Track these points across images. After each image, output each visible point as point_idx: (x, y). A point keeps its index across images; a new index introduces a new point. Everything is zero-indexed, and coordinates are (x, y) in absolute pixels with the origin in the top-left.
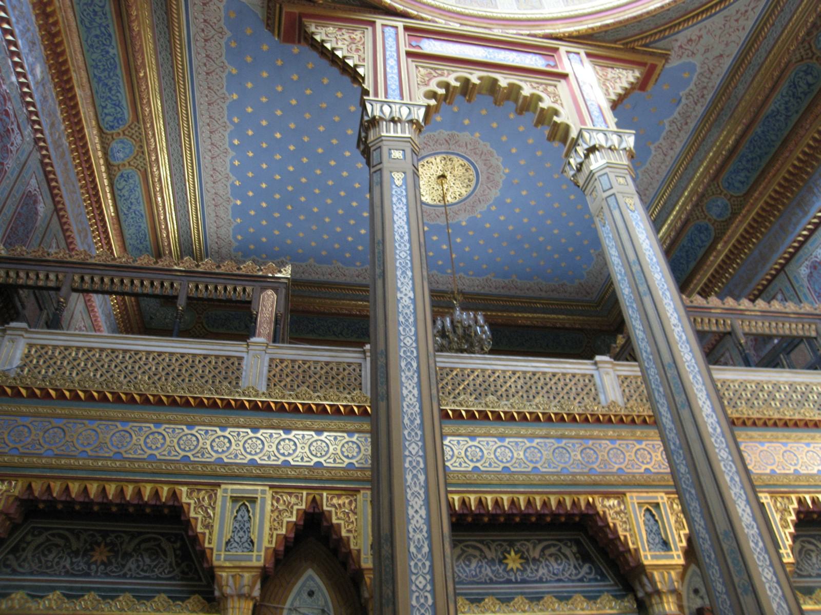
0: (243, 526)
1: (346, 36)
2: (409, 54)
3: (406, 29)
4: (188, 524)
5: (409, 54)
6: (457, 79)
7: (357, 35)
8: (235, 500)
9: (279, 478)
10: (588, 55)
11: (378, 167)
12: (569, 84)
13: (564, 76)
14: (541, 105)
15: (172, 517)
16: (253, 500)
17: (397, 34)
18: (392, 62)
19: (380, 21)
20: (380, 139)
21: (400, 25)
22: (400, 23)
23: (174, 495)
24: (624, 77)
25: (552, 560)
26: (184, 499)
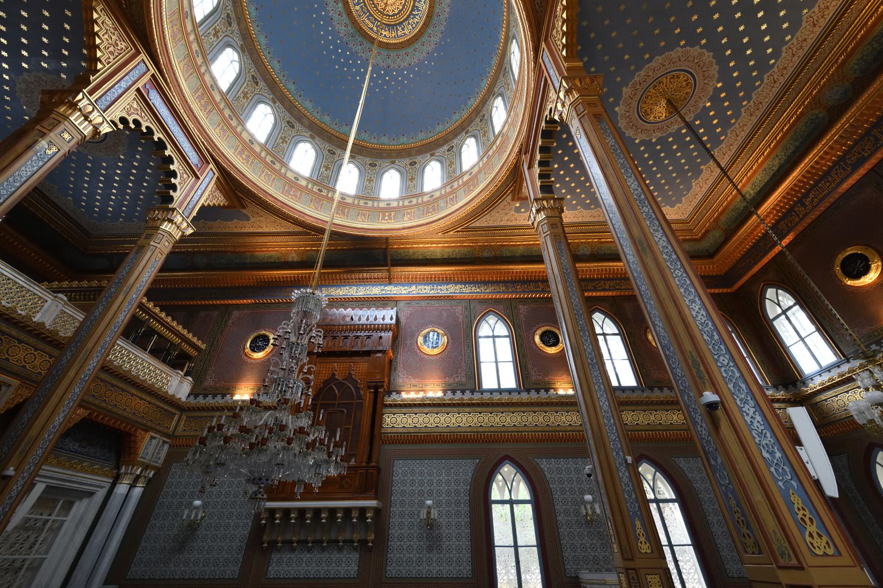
1: (114, 37)
2: (138, 90)
3: (153, 76)
5: (138, 90)
6: (147, 128)
7: (122, 45)
10: (218, 178)
11: (45, 131)
12: (195, 183)
13: (198, 178)
14: (172, 180)
17: (145, 73)
18: (123, 85)
19: (143, 56)
20: (66, 118)
21: (152, 71)
22: (153, 70)
24: (219, 200)
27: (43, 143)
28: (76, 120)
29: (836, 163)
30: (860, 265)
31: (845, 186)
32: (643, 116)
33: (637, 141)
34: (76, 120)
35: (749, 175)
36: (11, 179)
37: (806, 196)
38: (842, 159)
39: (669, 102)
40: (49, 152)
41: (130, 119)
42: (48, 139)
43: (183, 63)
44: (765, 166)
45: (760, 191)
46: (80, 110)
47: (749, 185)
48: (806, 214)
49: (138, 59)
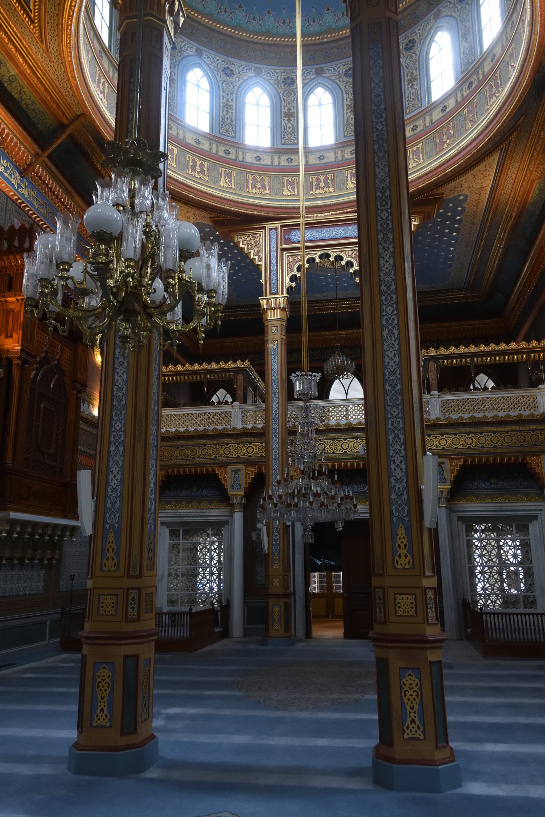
0: (236, 479)
2: (283, 250)
4: (219, 480)
8: (233, 471)
9: (248, 462)
15: (214, 476)
16: (240, 470)
18: (274, 261)
19: (269, 225)
22: (277, 225)
23: (213, 470)
25: (354, 484)
26: (217, 472)
27: (270, 345)
28: (271, 317)
34: (271, 317)
36: (273, 378)
40: (275, 347)
41: (295, 272)
42: (270, 342)
43: (285, 189)
46: (267, 309)
49: (267, 230)
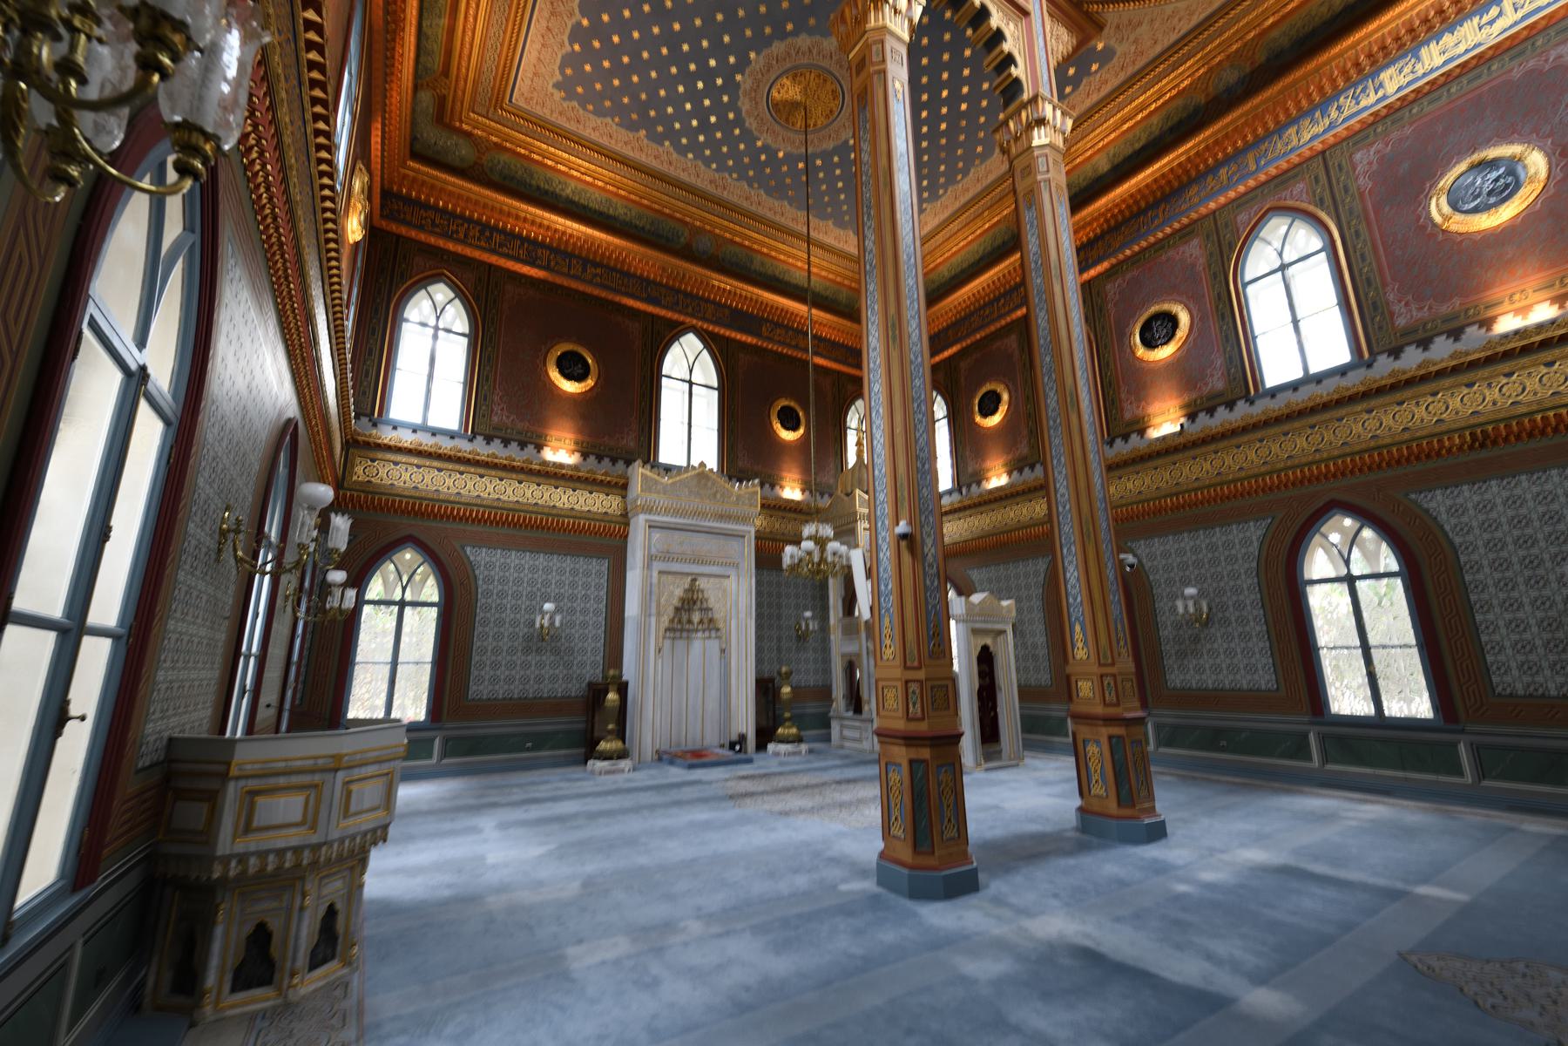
29: (641, 278)
30: (579, 370)
31: (631, 302)
32: (795, 74)
33: (752, 55)
35: (580, 172)
37: (596, 265)
38: (648, 281)
39: (794, 105)
44: (615, 200)
45: (572, 202)
47: (580, 186)
48: (575, 277)
